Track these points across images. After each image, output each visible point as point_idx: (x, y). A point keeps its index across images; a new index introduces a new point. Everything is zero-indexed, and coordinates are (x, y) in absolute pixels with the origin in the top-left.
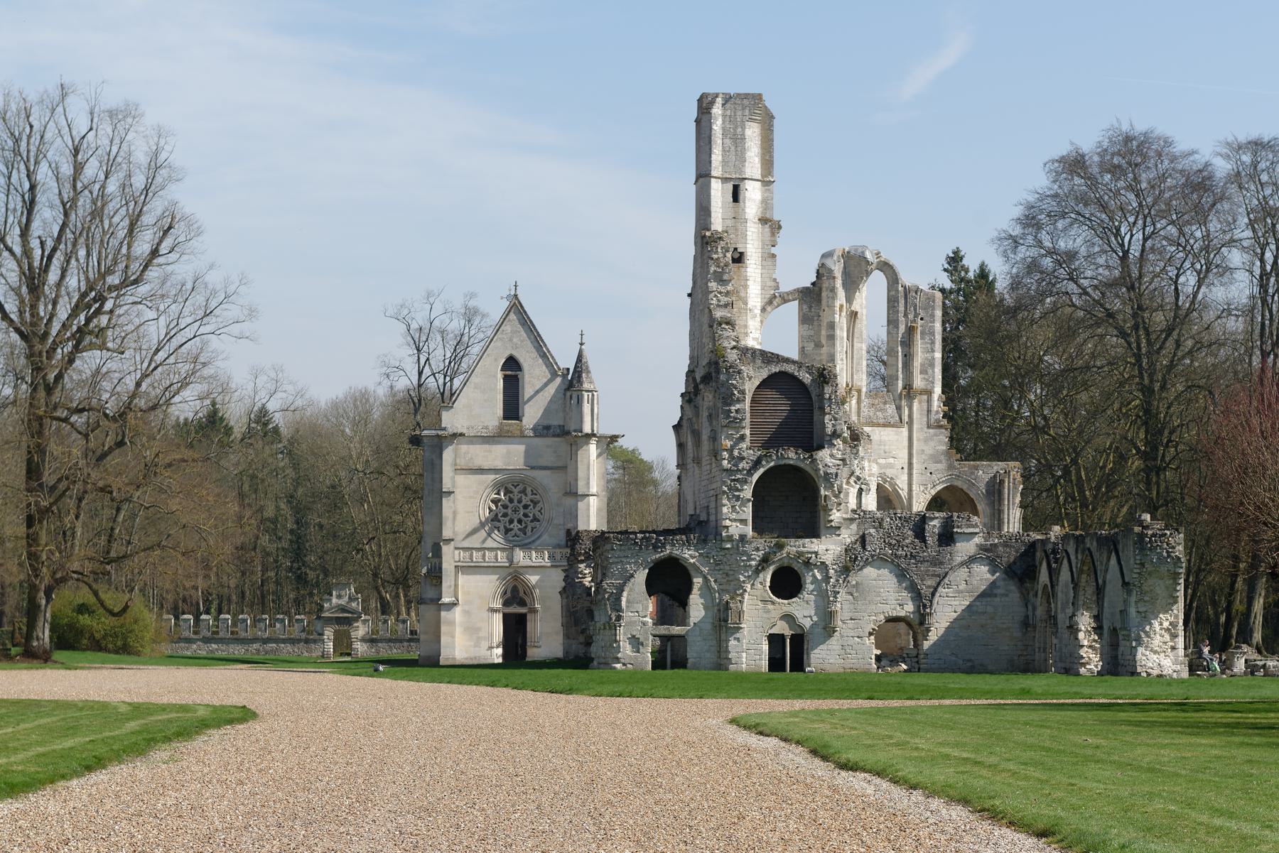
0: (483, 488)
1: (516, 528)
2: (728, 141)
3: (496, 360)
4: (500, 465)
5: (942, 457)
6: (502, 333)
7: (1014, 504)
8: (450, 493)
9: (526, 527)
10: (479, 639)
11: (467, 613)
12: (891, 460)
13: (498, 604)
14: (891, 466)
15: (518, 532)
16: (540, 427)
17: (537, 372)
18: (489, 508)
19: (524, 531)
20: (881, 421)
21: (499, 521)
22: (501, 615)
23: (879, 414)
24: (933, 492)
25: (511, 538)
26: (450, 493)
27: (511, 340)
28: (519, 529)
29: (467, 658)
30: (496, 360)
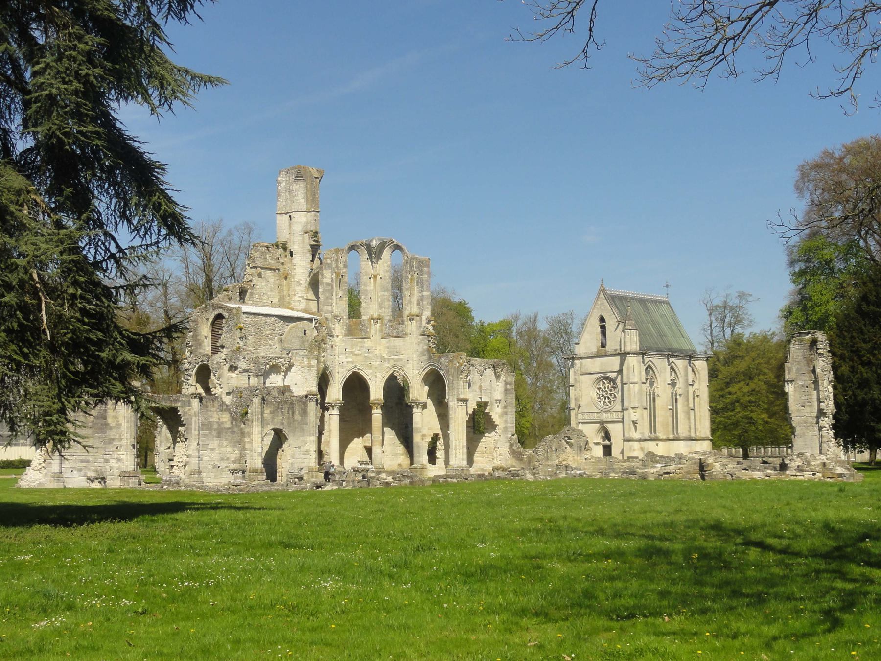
2: (287, 194)
4: (598, 370)
5: (426, 353)
7: (458, 377)
8: (573, 386)
12: (401, 357)
13: (601, 441)
14: (401, 360)
19: (610, 403)
20: (394, 335)
22: (601, 446)
23: (395, 331)
24: (424, 373)
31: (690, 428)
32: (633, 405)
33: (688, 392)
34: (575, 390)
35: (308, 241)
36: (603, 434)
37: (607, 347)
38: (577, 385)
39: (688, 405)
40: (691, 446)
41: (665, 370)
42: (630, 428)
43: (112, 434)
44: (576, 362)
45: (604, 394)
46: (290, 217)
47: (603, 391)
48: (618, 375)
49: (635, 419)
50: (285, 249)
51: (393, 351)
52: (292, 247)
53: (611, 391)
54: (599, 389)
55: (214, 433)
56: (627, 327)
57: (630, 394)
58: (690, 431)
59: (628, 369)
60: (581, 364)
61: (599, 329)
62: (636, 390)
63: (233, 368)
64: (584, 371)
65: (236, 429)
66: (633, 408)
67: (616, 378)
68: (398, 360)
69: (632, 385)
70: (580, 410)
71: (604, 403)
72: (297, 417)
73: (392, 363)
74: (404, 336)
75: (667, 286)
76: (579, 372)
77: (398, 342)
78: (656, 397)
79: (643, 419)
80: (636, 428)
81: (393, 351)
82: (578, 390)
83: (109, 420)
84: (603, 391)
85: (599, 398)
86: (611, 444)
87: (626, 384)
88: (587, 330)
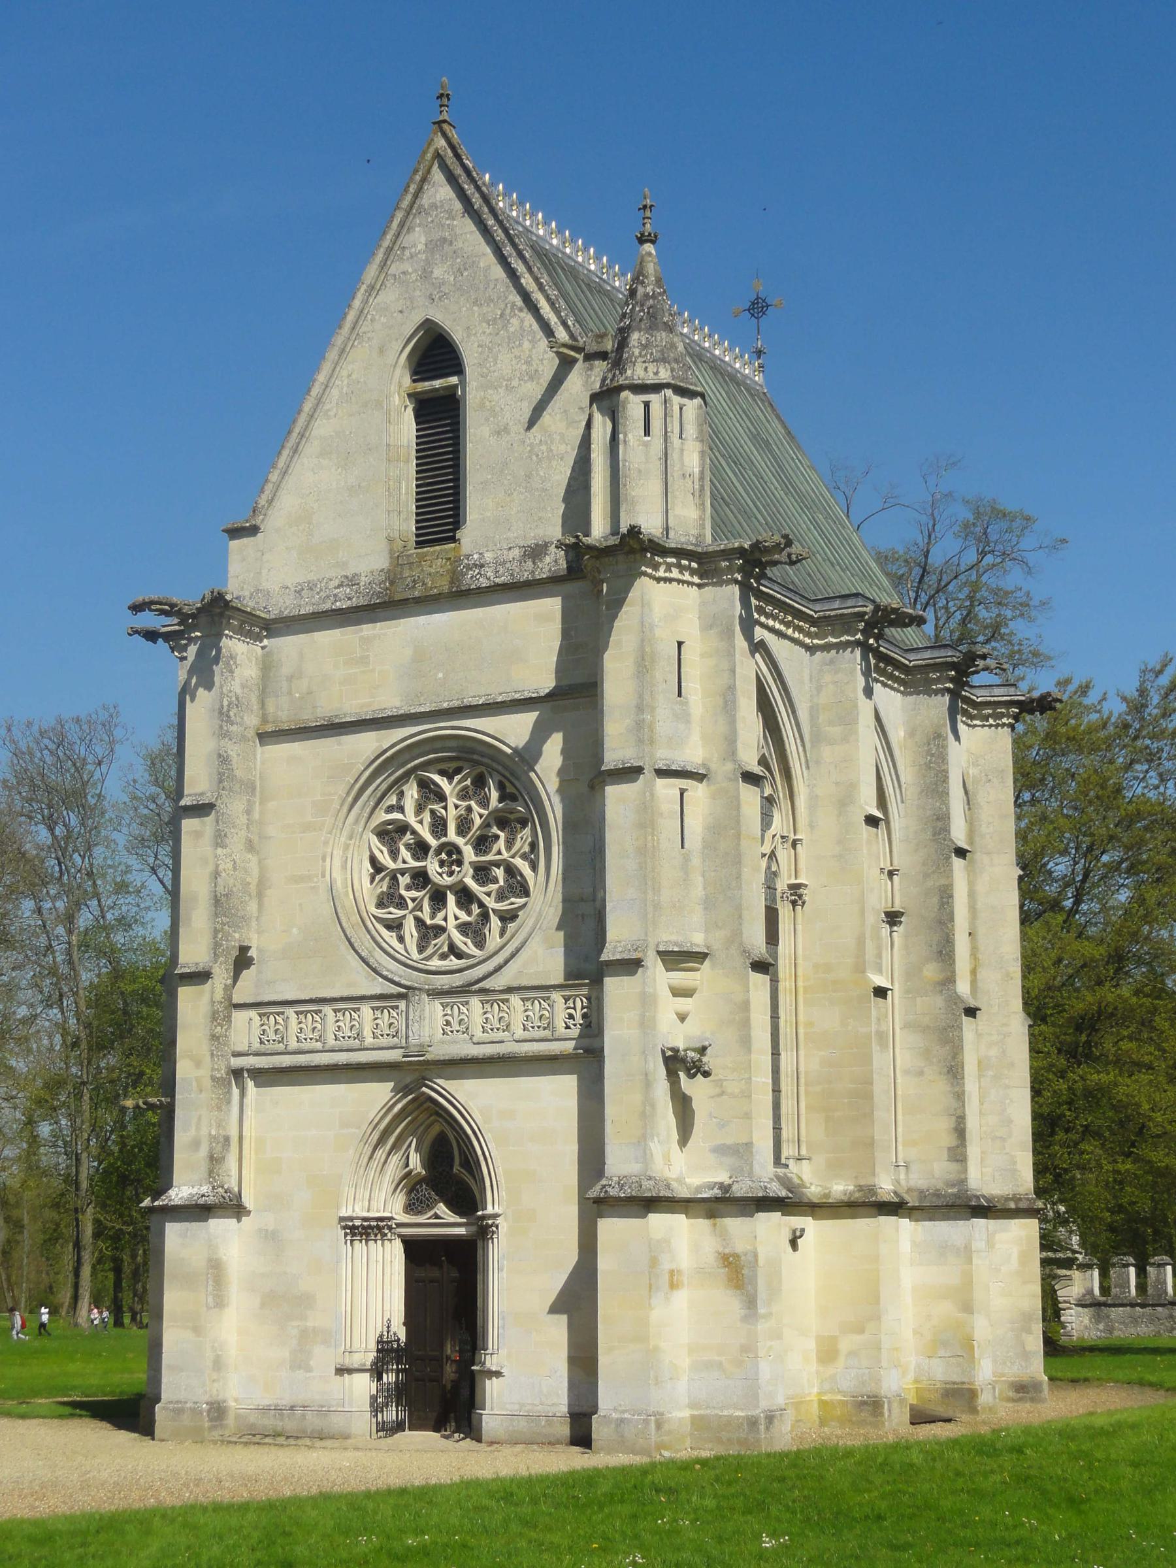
0: (342, 790)
1: (451, 924)
3: (382, 351)
4: (391, 702)
6: (401, 259)
8: (202, 809)
9: (485, 917)
10: (306, 1337)
11: (271, 1238)
13: (394, 1207)
15: (458, 938)
16: (516, 553)
17: (505, 363)
18: (373, 860)
21: (401, 903)
22: (397, 1248)
25: (435, 963)
26: (202, 809)
27: (426, 275)
28: (463, 928)
29: (266, 1409)
30: (382, 351)
31: (960, 1132)
32: (670, 938)
33: (946, 896)
34: (220, 840)
36: (416, 1162)
37: (469, 537)
38: (234, 807)
39: (949, 980)
40: (967, 1253)
41: (848, 720)
42: (646, 1115)
44: (234, 646)
45: (432, 866)
47: (421, 849)
48: (540, 734)
49: (680, 1038)
53: (482, 843)
54: (391, 834)
56: (638, 372)
57: (646, 853)
58: (958, 1154)
59: (644, 664)
60: (267, 666)
61: (407, 428)
62: (696, 824)
64: (283, 713)
66: (676, 958)
67: (529, 755)
69: (667, 789)
70: (247, 988)
71: (428, 933)
75: (758, 308)
76: (252, 721)
78: (785, 912)
79: (746, 1042)
80: (683, 1107)
82: (237, 840)
84: (421, 849)
85: (391, 898)
86: (484, 1231)
87: (630, 773)
88: (322, 428)
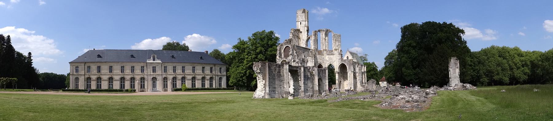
14: (332, 61)
24: (340, 64)
35: (306, 29)
43: (282, 78)
46: (301, 23)
50: (299, 31)
51: (330, 59)
52: (301, 30)
55: (307, 79)
63: (294, 61)
65: (311, 78)
68: (331, 61)
72: (324, 74)
73: (330, 62)
74: (333, 55)
77: (331, 56)
81: (330, 59)
83: (281, 73)
